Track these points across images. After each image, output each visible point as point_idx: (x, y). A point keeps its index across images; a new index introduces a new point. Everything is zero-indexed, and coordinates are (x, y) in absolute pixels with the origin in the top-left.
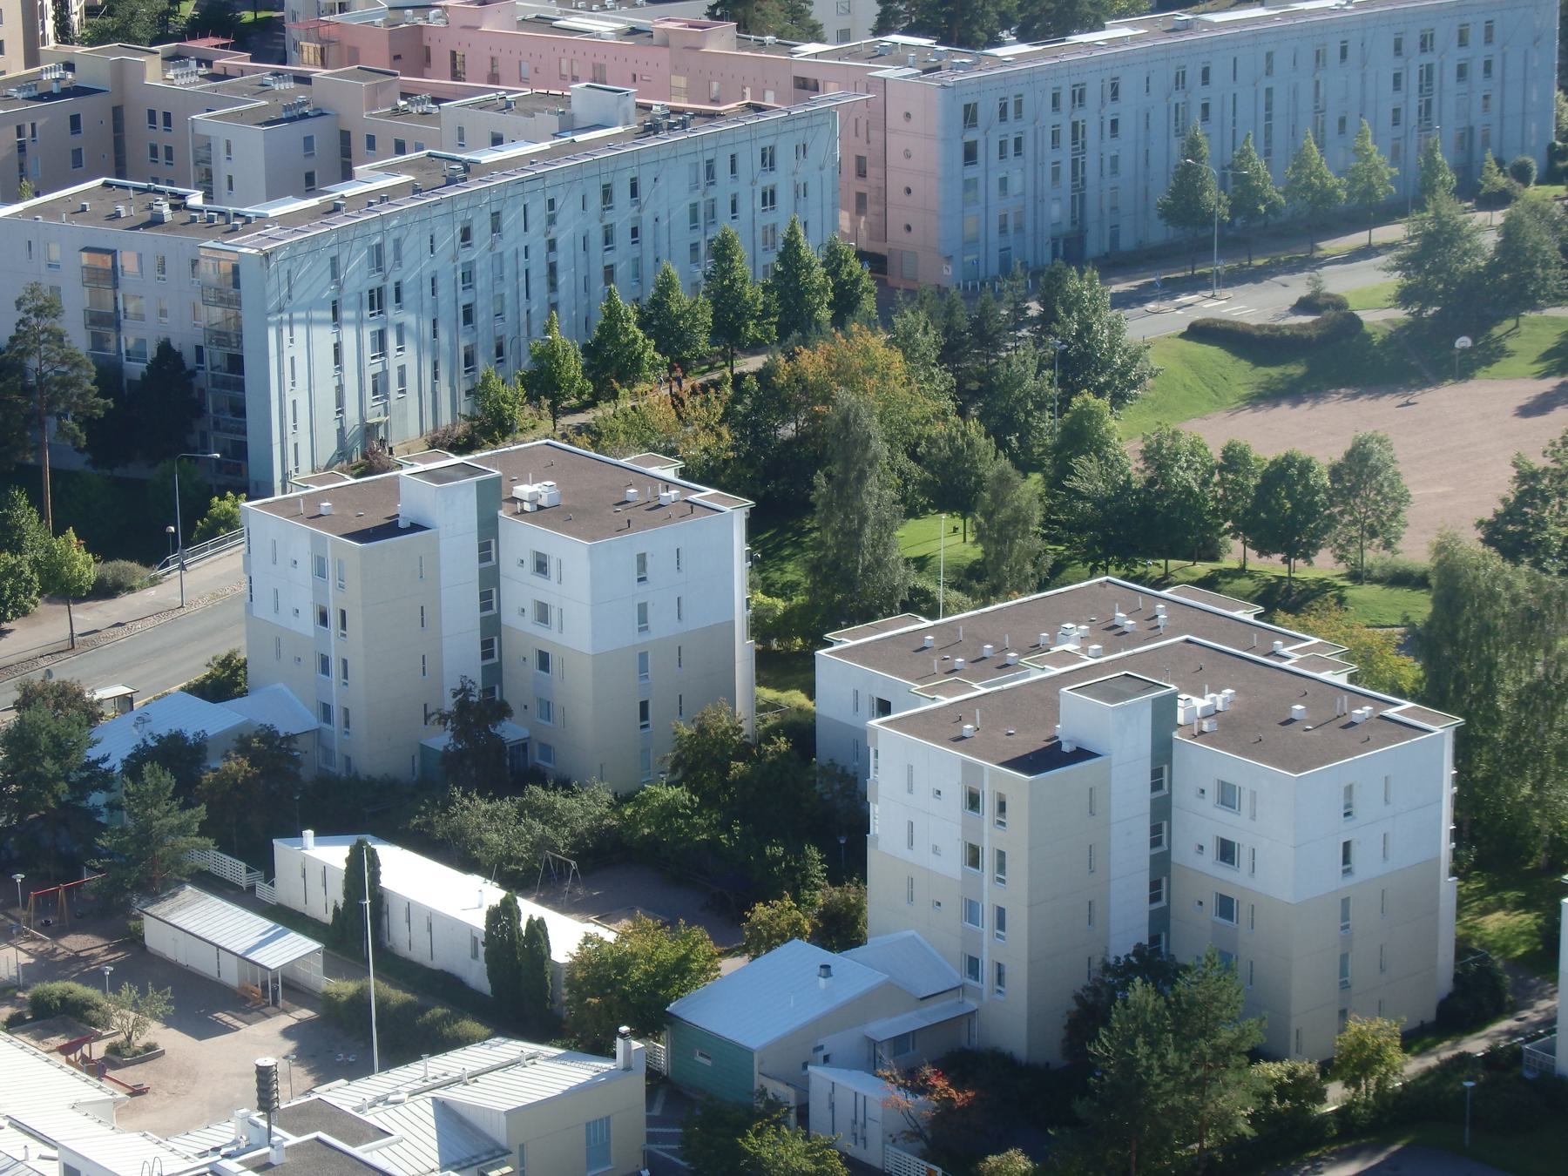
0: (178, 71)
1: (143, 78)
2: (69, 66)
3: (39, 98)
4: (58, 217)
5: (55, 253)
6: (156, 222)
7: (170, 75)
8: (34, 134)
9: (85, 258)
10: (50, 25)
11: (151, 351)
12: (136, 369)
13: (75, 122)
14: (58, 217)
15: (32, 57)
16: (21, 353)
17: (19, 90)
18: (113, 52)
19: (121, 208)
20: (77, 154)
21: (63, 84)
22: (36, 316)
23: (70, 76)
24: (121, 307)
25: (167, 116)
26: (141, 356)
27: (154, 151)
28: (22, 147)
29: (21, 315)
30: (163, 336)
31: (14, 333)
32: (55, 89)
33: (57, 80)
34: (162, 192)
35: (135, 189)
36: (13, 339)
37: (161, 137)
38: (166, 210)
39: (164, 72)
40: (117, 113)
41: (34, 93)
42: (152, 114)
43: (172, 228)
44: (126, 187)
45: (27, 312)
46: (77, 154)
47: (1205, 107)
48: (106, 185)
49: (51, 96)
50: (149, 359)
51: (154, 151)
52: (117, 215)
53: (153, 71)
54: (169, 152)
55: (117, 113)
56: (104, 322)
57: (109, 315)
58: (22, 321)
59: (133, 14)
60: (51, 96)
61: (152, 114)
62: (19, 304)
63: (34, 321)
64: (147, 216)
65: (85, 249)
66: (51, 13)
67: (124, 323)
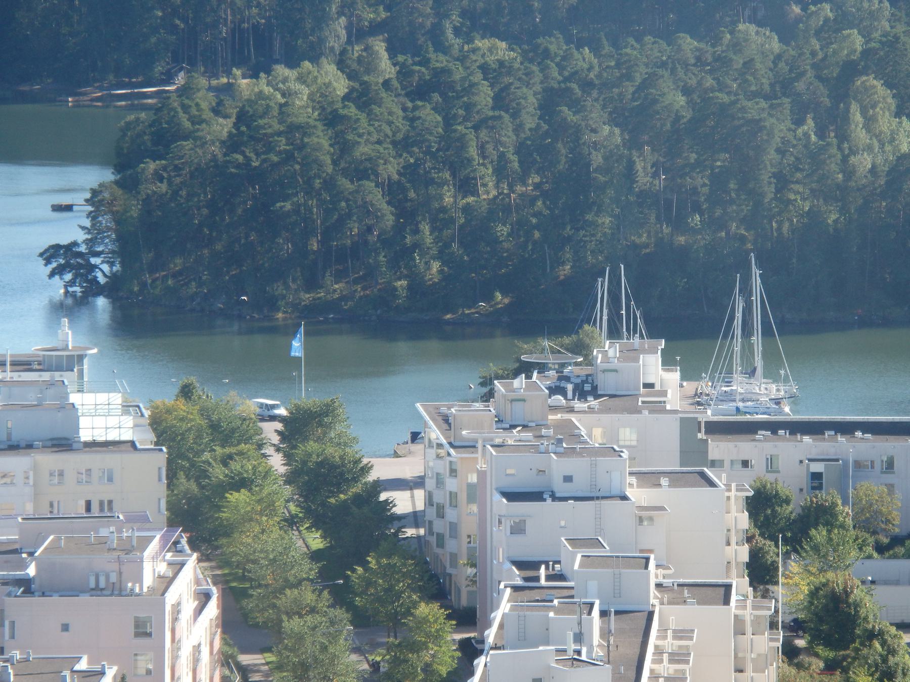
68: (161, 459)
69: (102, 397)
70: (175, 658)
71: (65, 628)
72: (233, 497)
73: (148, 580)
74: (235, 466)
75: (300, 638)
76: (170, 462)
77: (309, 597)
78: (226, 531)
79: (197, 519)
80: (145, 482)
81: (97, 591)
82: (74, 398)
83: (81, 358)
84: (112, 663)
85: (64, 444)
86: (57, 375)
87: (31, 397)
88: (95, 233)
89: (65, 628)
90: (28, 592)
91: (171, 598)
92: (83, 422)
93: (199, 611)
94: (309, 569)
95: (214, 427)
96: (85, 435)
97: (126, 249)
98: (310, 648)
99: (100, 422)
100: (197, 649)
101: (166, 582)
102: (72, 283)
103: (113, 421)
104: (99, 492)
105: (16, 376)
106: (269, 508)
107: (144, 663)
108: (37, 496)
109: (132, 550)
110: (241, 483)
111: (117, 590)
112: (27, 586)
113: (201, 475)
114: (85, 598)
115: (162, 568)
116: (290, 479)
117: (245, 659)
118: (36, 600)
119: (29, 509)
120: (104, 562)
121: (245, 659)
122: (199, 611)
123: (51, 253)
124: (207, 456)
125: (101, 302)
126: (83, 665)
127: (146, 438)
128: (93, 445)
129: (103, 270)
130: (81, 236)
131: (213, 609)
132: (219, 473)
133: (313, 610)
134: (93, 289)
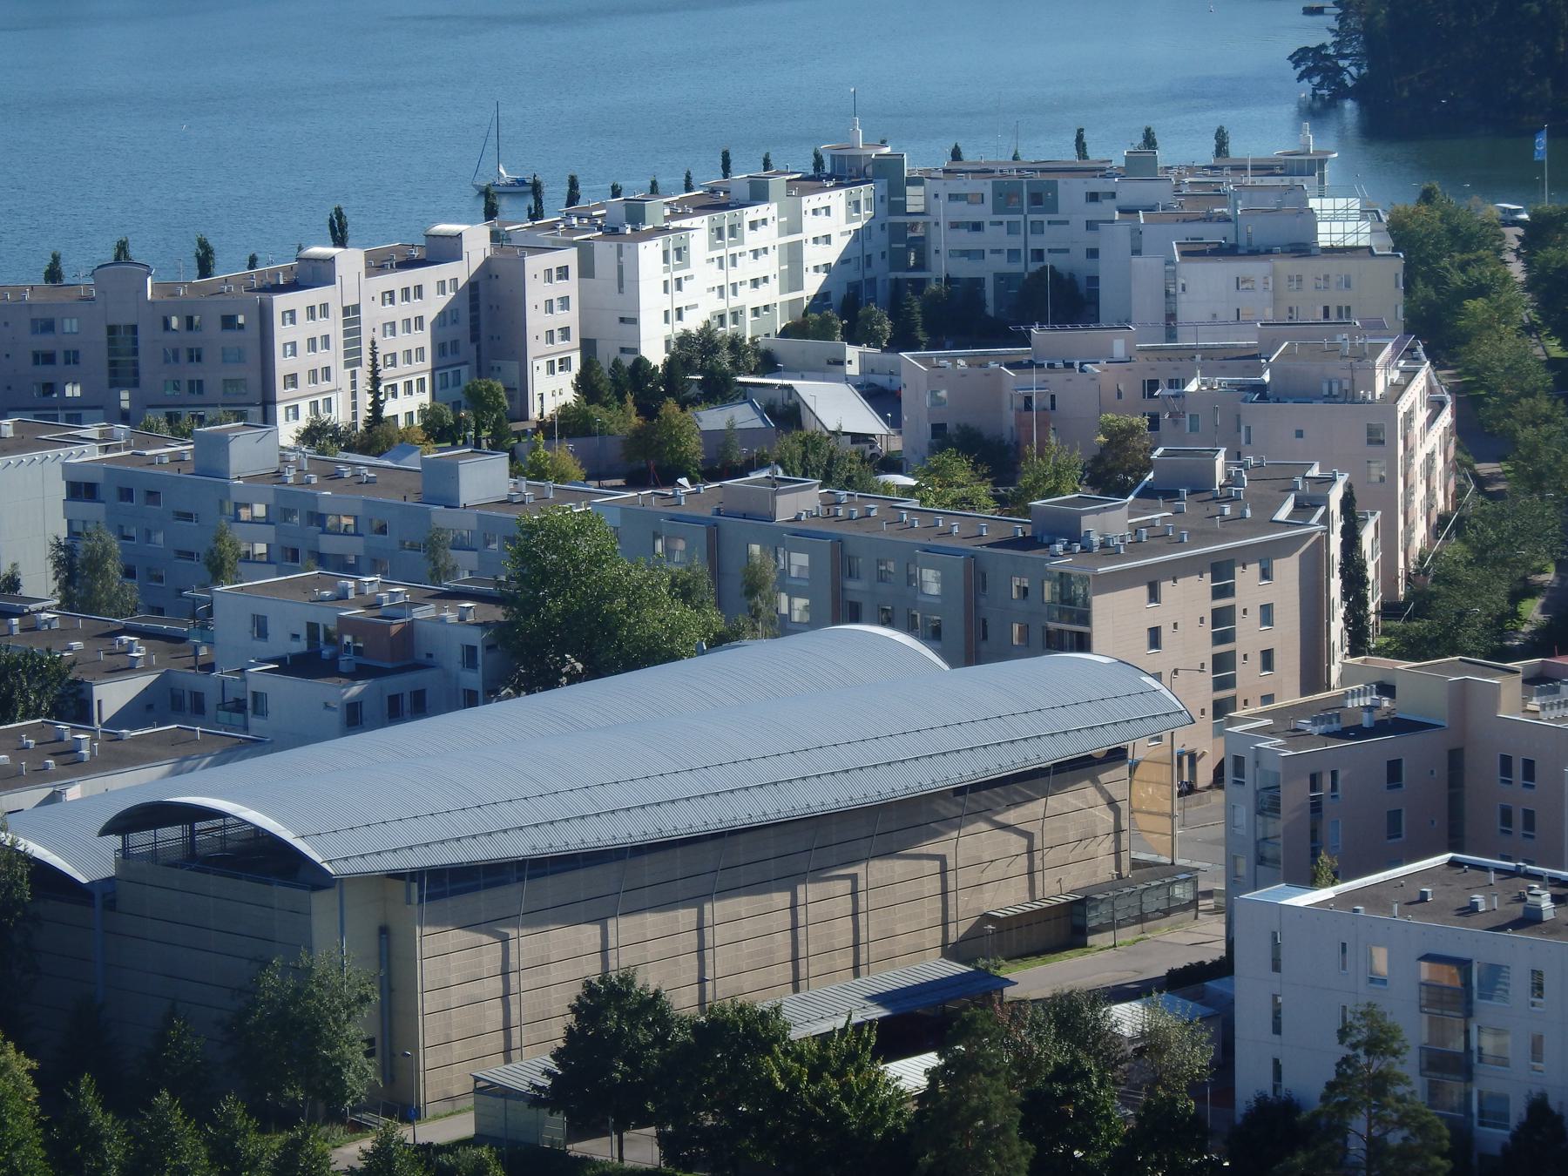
0: (1544, 699)
1: (1495, 705)
2: (1386, 689)
3: (1343, 734)
4: (1387, 908)
5: (1381, 960)
6: (1530, 919)
7: (1534, 704)
8: (1334, 787)
9: (1426, 971)
10: (1337, 627)
11: (1517, 1111)
12: (1494, 1138)
13: (1394, 768)
14: (1387, 908)
15: (1313, 674)
16: (1342, 1107)
17: (1315, 722)
18: (1451, 669)
19: (1478, 898)
20: (1394, 817)
21: (1378, 715)
22: (1368, 1053)
23: (1386, 703)
24: (1474, 1045)
25: (1529, 766)
26: (1500, 1119)
27: (1506, 816)
28: (1316, 806)
29: (1346, 1051)
30: (1536, 1090)
31: (1332, 1077)
32: (1366, 720)
33: (1369, 709)
34: (1537, 877)
35: (1498, 871)
36: (1331, 1086)
37: (1517, 796)
38: (1546, 903)
39: (1525, 701)
40: (1456, 759)
41: (1336, 727)
42: (1506, 762)
43: (1554, 929)
44: (1484, 868)
45: (1354, 1046)
46: (1394, 817)
47: (1537, 975)
48: (1453, 863)
49: (1359, 732)
50: (1513, 1123)
51: (1506, 816)
52: (1472, 908)
53: (1510, 698)
54: (1529, 816)
55: (1456, 759)
56: (1451, 1065)
57: (1455, 1055)
58: (1346, 1060)
59: (1461, 615)
60: (1359, 732)
61: (1506, 762)
62: (1343, 1034)
63: (1363, 1060)
64: (1518, 910)
65: (1427, 958)
66: (1339, 612)
67: (1479, 1069)
68: (1398, 264)
69: (1341, 203)
70: (1408, 465)
71: (1300, 434)
72: (1470, 304)
73: (1380, 388)
74: (1474, 272)
75: (1534, 448)
76: (1407, 268)
77: (1544, 406)
78: (1464, 338)
79: (1434, 330)
80: (1382, 290)
81: (1330, 398)
82: (1314, 203)
83: (1322, 163)
84: (1342, 471)
85: (1303, 248)
86: (1297, 180)
87: (1271, 202)
88: (1343, 35)
89: (1300, 434)
90: (1264, 398)
91: (1403, 406)
92: (1322, 227)
93: (1431, 420)
94: (1546, 378)
95: (1454, 231)
96: (1323, 240)
97: (1374, 50)
98: (1546, 457)
99: (1337, 227)
100: (1430, 457)
101: (1398, 390)
102: (1320, 86)
103: (1350, 227)
104: (1336, 298)
105: (1258, 181)
106: (1506, 313)
107: (1376, 472)
108: (1276, 301)
109: (1364, 358)
110: (1481, 291)
111: (1349, 397)
112: (1262, 391)
113: (1437, 280)
114: (1318, 406)
115: (1395, 375)
116: (1530, 286)
117: (1485, 468)
118: (1271, 406)
119: (1269, 314)
120: (1336, 369)
121: (1485, 468)
122: (1431, 420)
123: (1299, 57)
124: (1445, 262)
125: (1349, 105)
126: (1315, 472)
127: (1384, 244)
128: (1331, 250)
129: (1351, 72)
130: (1329, 39)
131: (1446, 418)
132: (1457, 278)
133: (1548, 419)
134: (1341, 93)
